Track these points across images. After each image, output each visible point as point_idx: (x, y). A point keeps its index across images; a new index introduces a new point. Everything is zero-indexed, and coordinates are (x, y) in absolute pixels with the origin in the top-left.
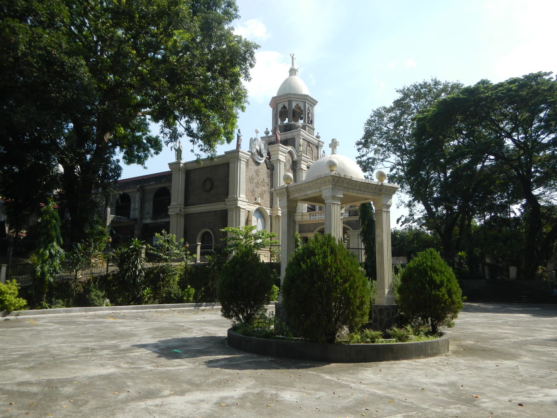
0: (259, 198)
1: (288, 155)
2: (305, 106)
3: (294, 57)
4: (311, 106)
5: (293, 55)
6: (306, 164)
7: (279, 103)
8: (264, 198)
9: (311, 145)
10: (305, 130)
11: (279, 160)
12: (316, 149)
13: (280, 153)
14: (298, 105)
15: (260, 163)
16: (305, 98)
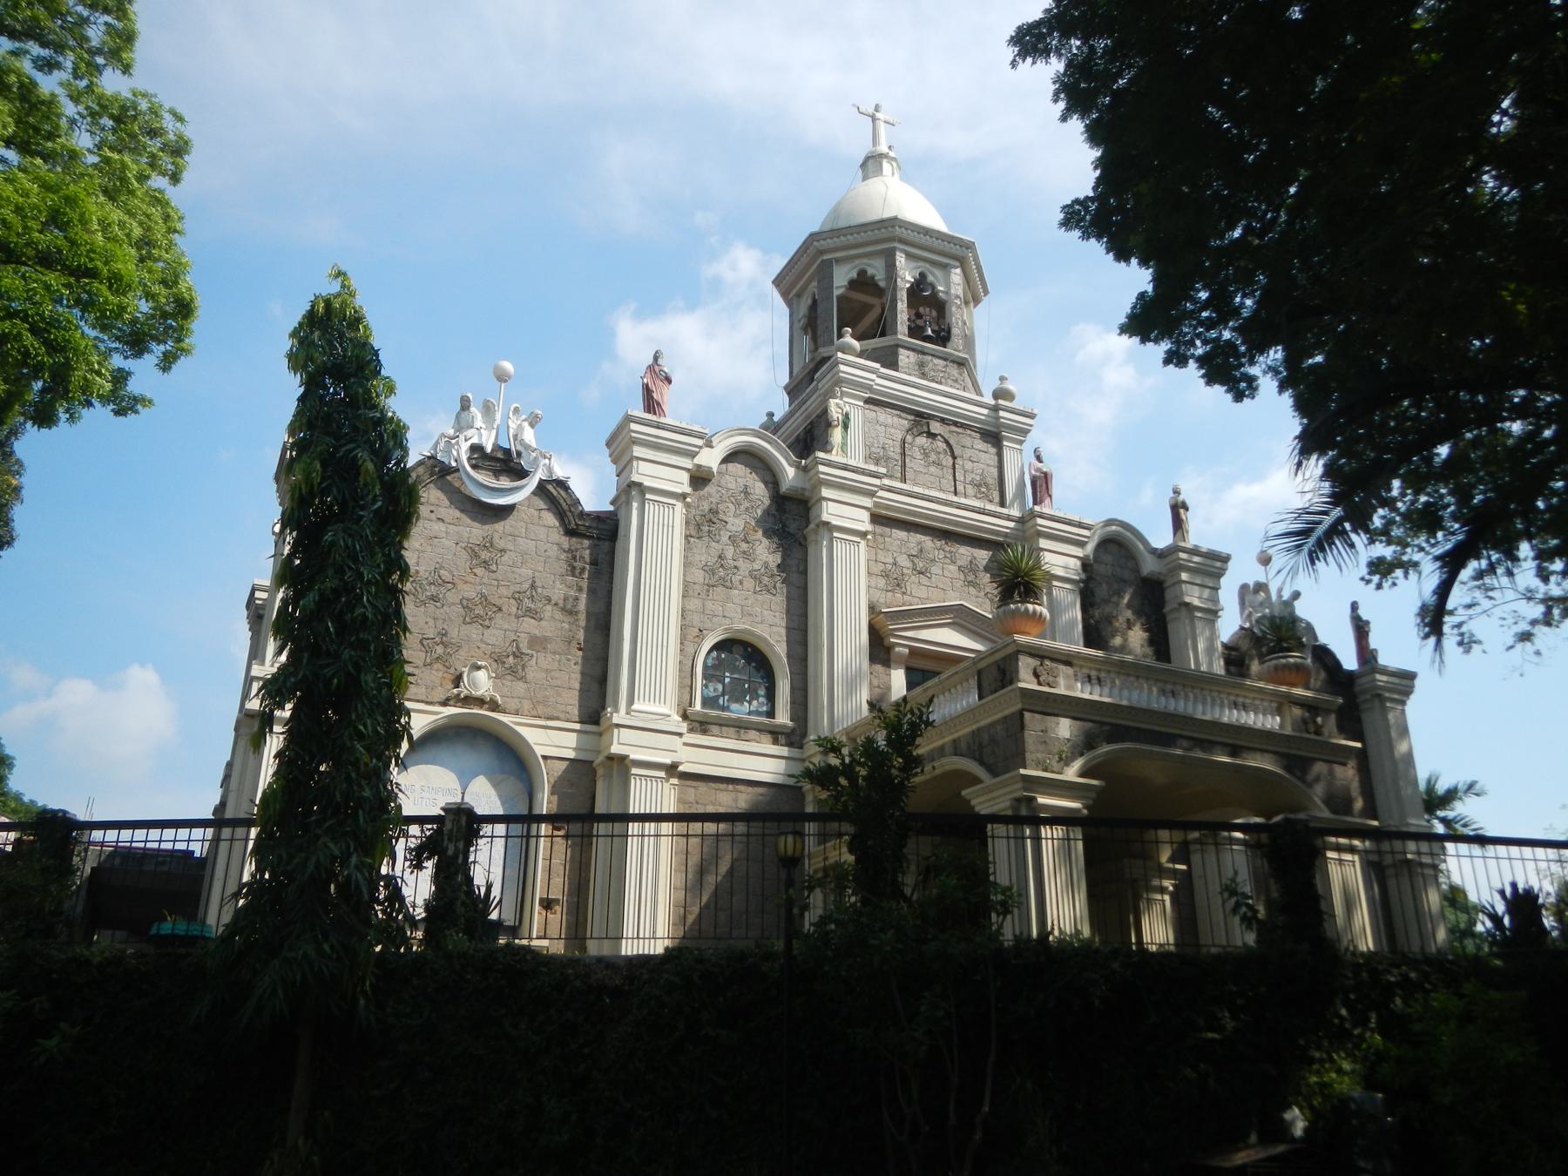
0: (481, 675)
1: (737, 468)
2: (891, 267)
4: (945, 267)
5: (877, 108)
6: (868, 502)
7: (799, 295)
8: (532, 673)
9: (936, 427)
10: (892, 364)
11: (640, 485)
12: (980, 444)
13: (638, 451)
14: (862, 273)
15: (508, 510)
16: (884, 233)
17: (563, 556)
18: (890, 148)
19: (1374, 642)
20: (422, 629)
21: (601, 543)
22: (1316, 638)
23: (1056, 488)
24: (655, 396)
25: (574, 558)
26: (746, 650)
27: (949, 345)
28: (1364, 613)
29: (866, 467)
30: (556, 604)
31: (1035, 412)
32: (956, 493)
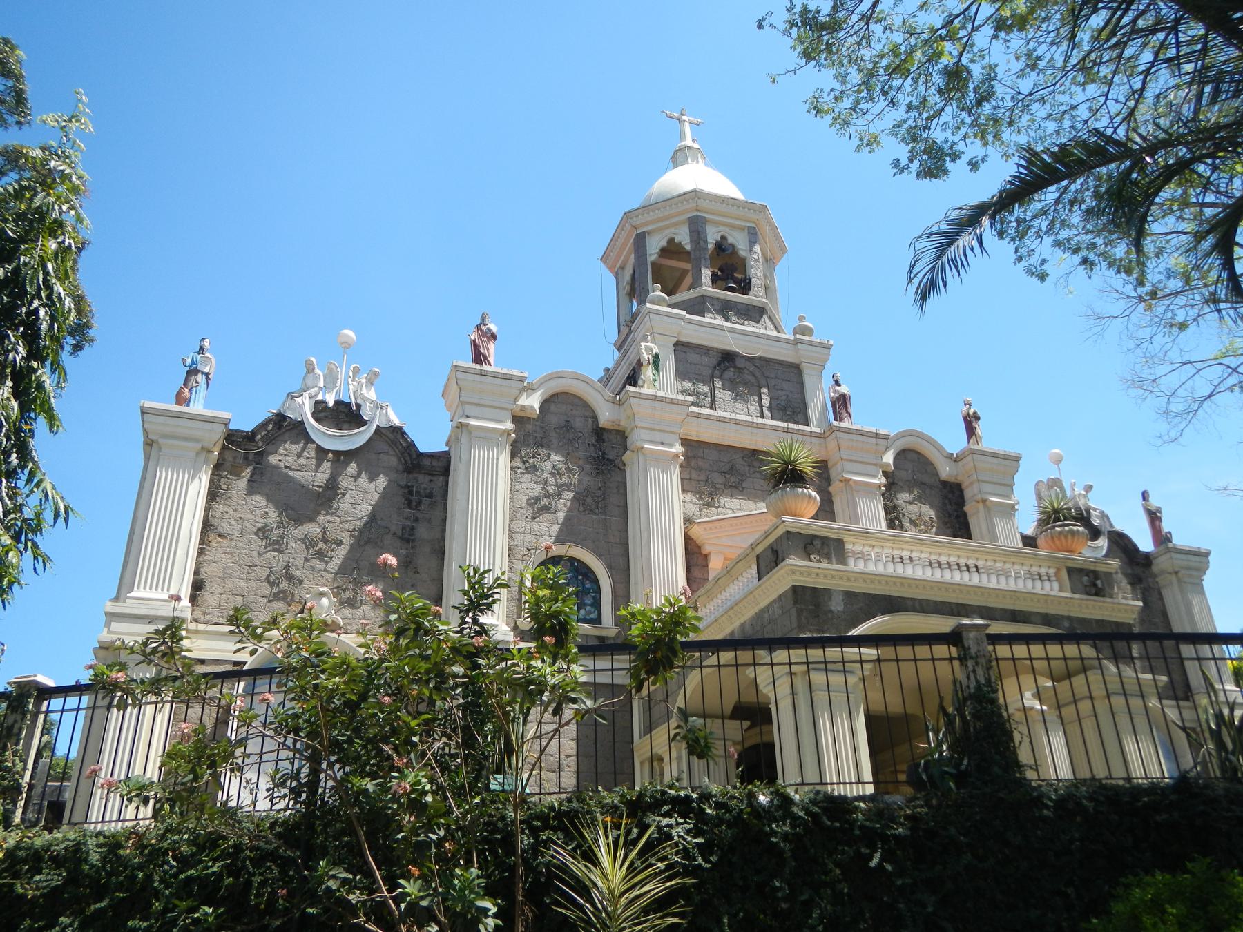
3: (684, 118)
7: (622, 268)
9: (740, 363)
14: (671, 241)
17: (401, 492)
18: (694, 141)
19: (1166, 526)
20: (270, 563)
21: (435, 478)
22: (1111, 526)
23: (853, 408)
24: (482, 350)
25: (411, 493)
26: (572, 564)
27: (751, 292)
28: (1154, 502)
29: (674, 397)
30: (395, 534)
31: (831, 342)
32: (762, 417)
